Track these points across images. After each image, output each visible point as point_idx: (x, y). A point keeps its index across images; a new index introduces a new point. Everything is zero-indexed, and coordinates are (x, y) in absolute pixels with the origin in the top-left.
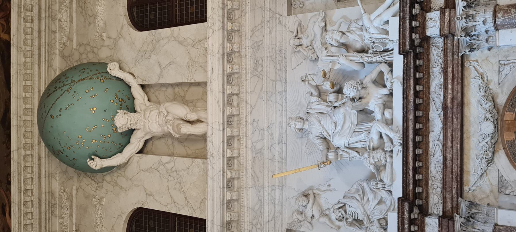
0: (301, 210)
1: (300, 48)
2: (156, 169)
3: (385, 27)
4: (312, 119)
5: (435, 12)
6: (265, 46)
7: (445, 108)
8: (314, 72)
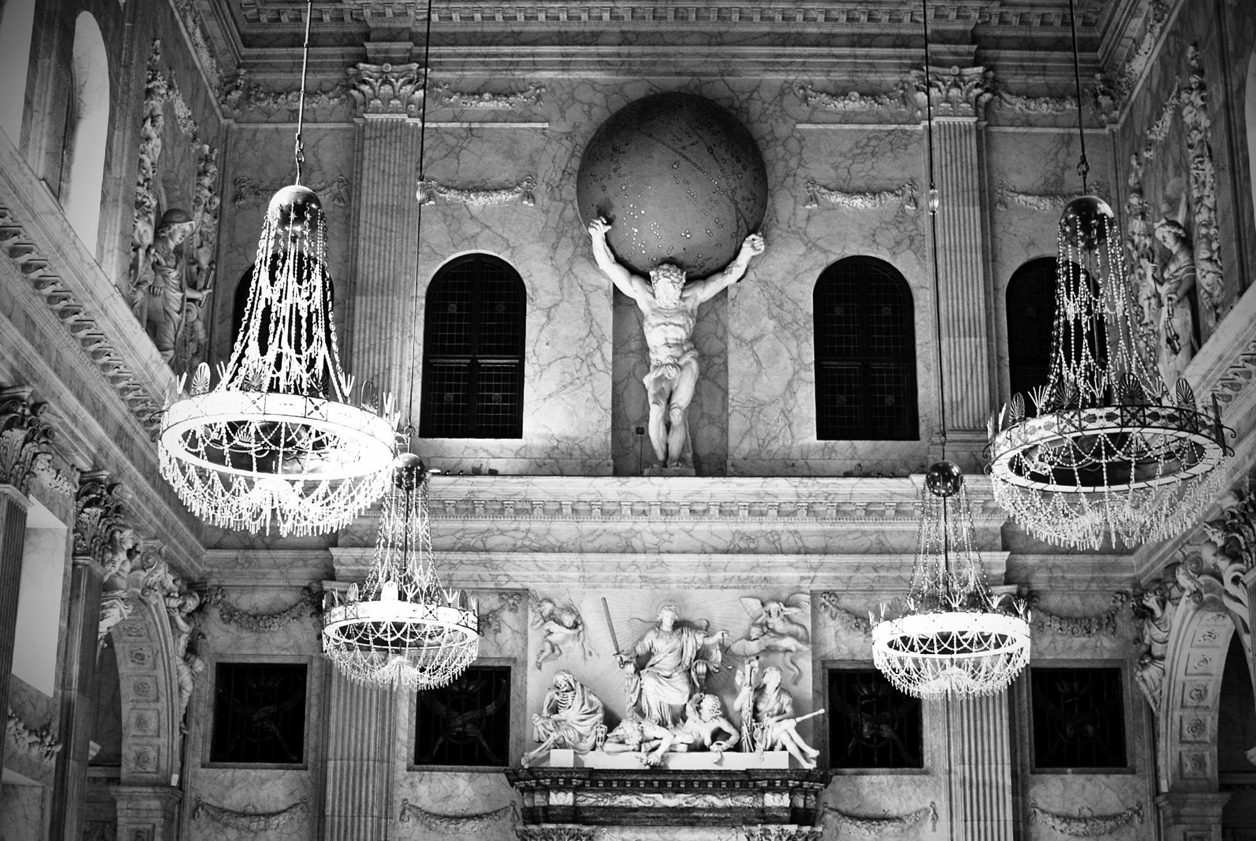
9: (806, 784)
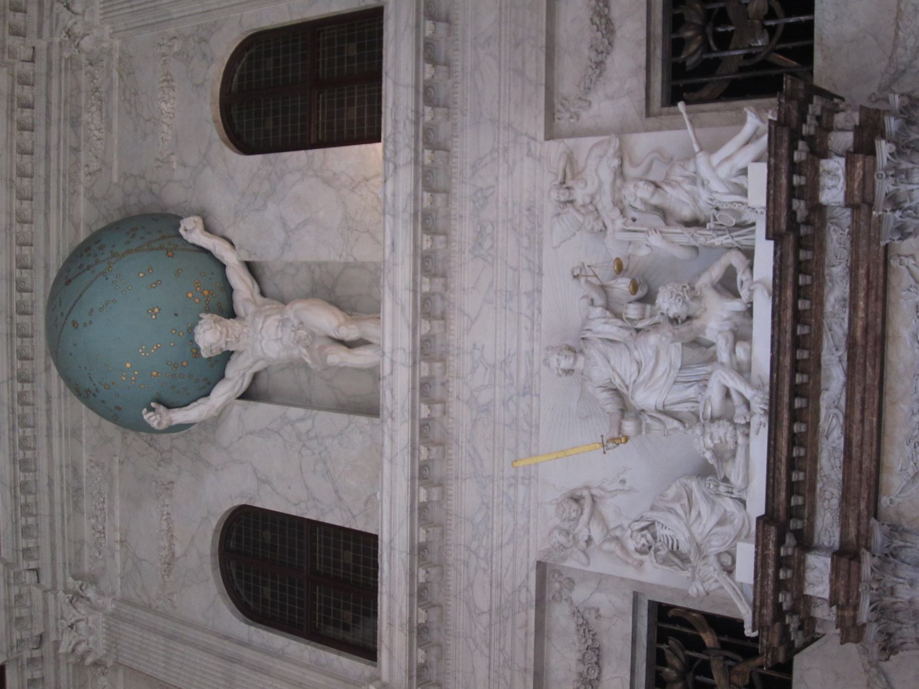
0: (566, 525)
1: (570, 208)
2: (278, 432)
3: (741, 180)
4: (594, 352)
5: (837, 159)
6: (500, 199)
7: (851, 344)
8: (599, 255)
9: (807, 129)
